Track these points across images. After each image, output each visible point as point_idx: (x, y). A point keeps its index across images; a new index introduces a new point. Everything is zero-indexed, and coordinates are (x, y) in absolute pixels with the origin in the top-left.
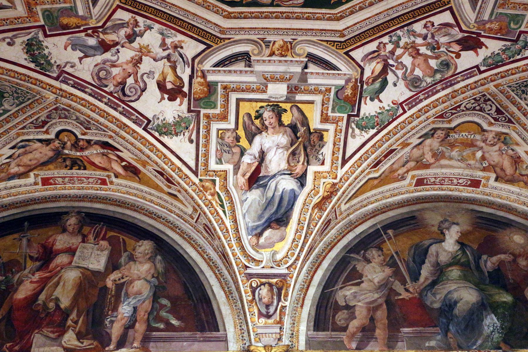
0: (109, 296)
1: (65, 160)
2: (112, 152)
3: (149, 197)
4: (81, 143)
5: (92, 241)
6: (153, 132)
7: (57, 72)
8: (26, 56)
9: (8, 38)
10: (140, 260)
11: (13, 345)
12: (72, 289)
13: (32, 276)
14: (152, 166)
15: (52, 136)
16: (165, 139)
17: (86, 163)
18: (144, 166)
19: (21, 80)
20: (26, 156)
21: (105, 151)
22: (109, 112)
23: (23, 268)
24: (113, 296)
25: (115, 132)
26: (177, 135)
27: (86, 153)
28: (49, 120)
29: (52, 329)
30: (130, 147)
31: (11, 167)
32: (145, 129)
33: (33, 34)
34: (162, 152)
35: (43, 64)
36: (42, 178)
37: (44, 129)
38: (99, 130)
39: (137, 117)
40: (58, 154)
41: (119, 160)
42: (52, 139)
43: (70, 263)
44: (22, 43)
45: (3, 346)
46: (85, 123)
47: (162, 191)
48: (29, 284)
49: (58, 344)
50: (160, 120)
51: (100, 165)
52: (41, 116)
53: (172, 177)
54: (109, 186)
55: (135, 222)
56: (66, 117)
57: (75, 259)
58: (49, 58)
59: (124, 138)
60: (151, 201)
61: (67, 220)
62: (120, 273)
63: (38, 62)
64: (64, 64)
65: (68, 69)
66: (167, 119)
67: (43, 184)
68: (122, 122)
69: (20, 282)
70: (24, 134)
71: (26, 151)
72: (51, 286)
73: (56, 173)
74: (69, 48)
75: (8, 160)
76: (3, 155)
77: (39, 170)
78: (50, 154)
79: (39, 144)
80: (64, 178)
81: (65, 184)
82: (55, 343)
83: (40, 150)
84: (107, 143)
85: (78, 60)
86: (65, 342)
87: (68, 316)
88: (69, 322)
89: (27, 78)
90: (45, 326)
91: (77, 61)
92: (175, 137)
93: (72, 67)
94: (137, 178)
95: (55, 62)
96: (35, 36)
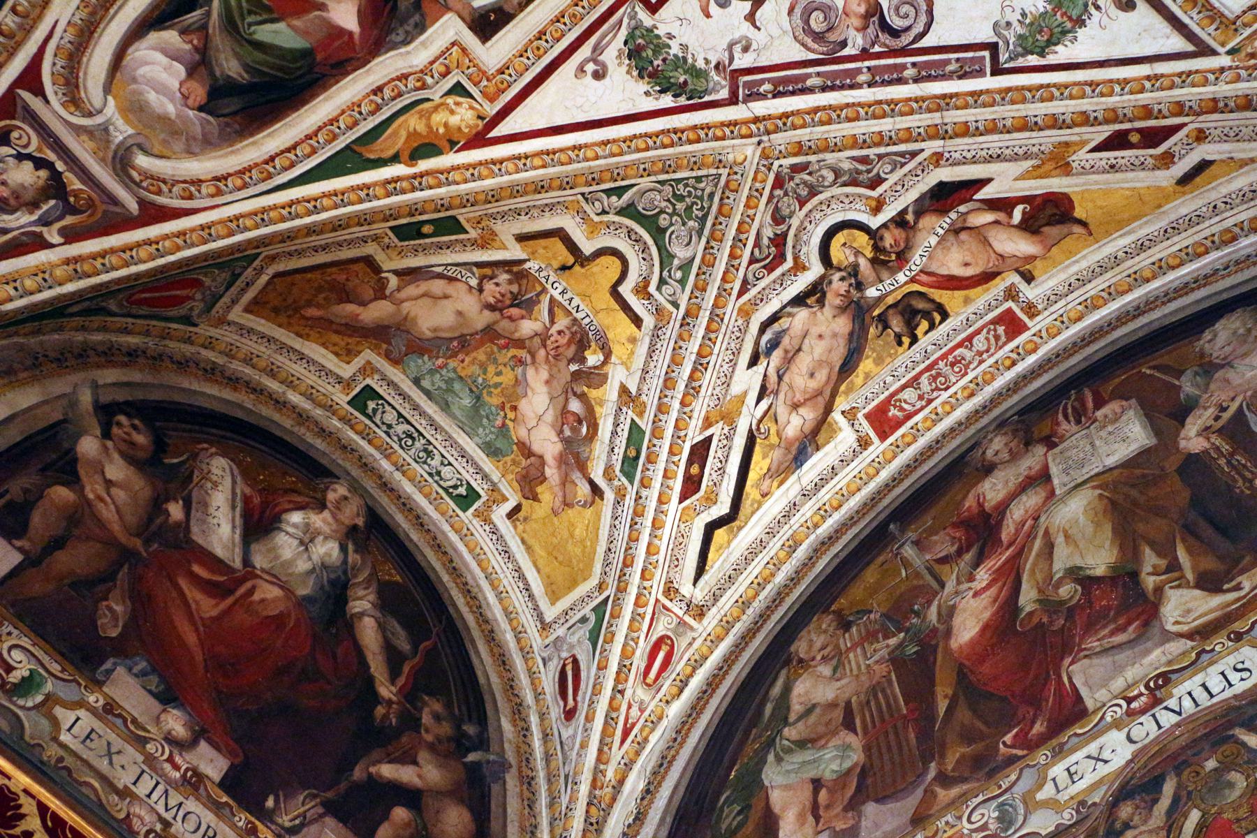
0: (1222, 462)
1: (883, 321)
2: (970, 206)
3: (1144, 261)
4: (888, 241)
5: (1074, 428)
6: (1020, 62)
7: (724, 83)
8: (643, 86)
9: (587, 61)
10: (1240, 351)
11: (1021, 730)
12: (1097, 525)
13: (970, 585)
14: (1083, 143)
15: (816, 270)
16: (1062, 53)
17: (937, 295)
18: (1065, 169)
19: (664, 146)
20: (793, 368)
21: (953, 215)
22: (889, 97)
23: (935, 585)
24: (1232, 455)
25: (935, 133)
26: (1081, 23)
27: (917, 260)
28: (783, 227)
29: (1112, 626)
30: (994, 142)
31: (782, 418)
32: (997, 71)
33: (626, 21)
34: (1075, 84)
35: (685, 82)
36: (867, 417)
37: (789, 263)
38: (903, 165)
39: (958, 60)
40: (858, 310)
41: (1001, 216)
42: (822, 278)
43: (1052, 493)
44: (619, 57)
45: (998, 750)
46: (858, 172)
47: (1160, 199)
48: (972, 601)
49: (1156, 639)
50: (1015, 24)
51: (969, 272)
52: (761, 226)
53: (1147, 112)
54: (1035, 325)
55: (1156, 326)
56: (813, 193)
57: (1056, 482)
58: (690, 61)
59: (965, 131)
60: (1161, 268)
61: (984, 453)
62: (1205, 408)
63: (673, 84)
64: (727, 54)
65: (742, 61)
66: (1029, 9)
67: (883, 436)
68: (936, 97)
69: (948, 614)
70: (755, 304)
71: (786, 352)
72: (1035, 564)
73: (889, 380)
74: (713, 8)
75: (764, 405)
76: (745, 393)
77: (847, 393)
78: (843, 325)
79: (802, 314)
80: (914, 382)
81: (930, 401)
82: (1149, 644)
83: (815, 331)
84: (941, 185)
85: (748, 24)
86: (1177, 623)
87: (1134, 575)
88: (1150, 582)
89: (673, 135)
90: (1082, 638)
91: (746, 29)
92: (1081, 33)
93: (746, 49)
94: (1077, 229)
95: (707, 61)
96: (633, 22)
